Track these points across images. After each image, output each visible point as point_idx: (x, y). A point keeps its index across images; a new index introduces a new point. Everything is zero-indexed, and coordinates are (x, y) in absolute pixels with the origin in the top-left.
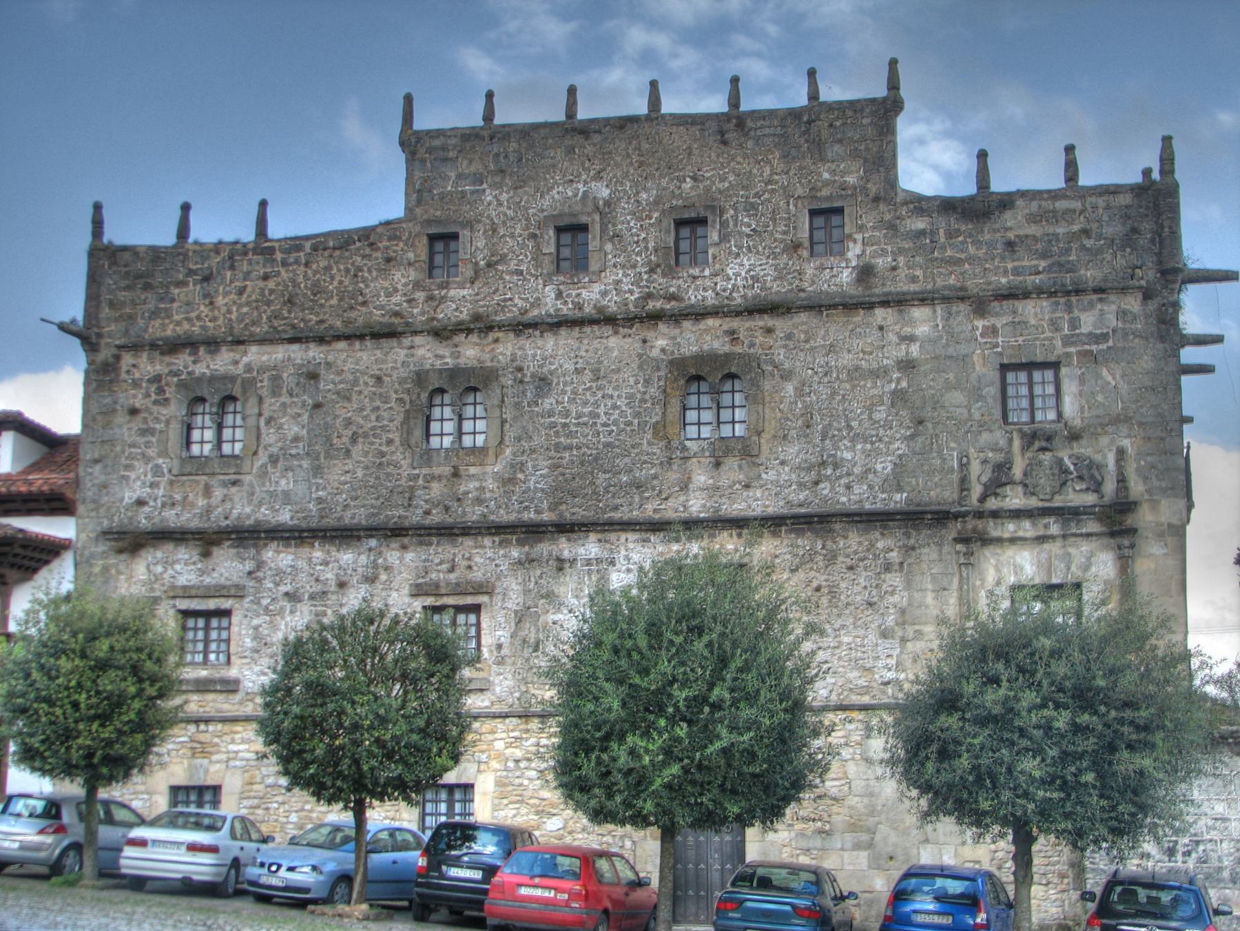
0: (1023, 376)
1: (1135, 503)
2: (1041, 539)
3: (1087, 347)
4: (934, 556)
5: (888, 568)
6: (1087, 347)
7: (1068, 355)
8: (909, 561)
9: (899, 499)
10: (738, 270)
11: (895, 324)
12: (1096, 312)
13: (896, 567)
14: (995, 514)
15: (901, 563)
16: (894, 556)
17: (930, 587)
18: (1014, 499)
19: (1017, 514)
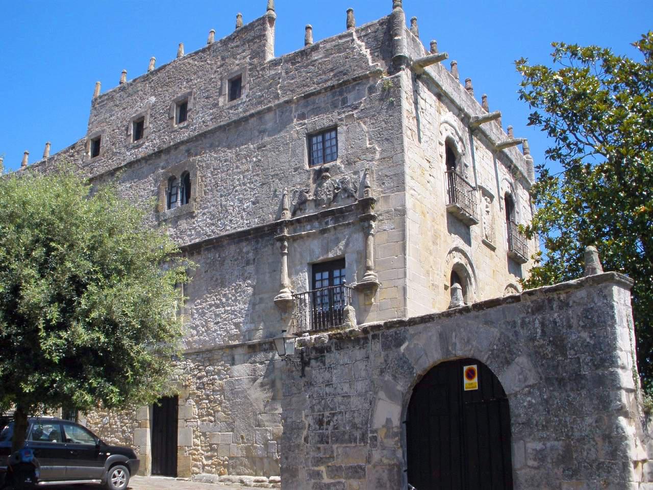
0: (320, 138)
1: (372, 199)
2: (324, 231)
3: (351, 113)
4: (270, 252)
5: (248, 263)
6: (351, 113)
7: (341, 120)
8: (258, 257)
9: (255, 223)
10: (201, 119)
11: (258, 125)
12: (356, 91)
13: (252, 262)
14: (298, 221)
15: (254, 259)
16: (251, 256)
17: (267, 271)
18: (310, 212)
19: (309, 219)
